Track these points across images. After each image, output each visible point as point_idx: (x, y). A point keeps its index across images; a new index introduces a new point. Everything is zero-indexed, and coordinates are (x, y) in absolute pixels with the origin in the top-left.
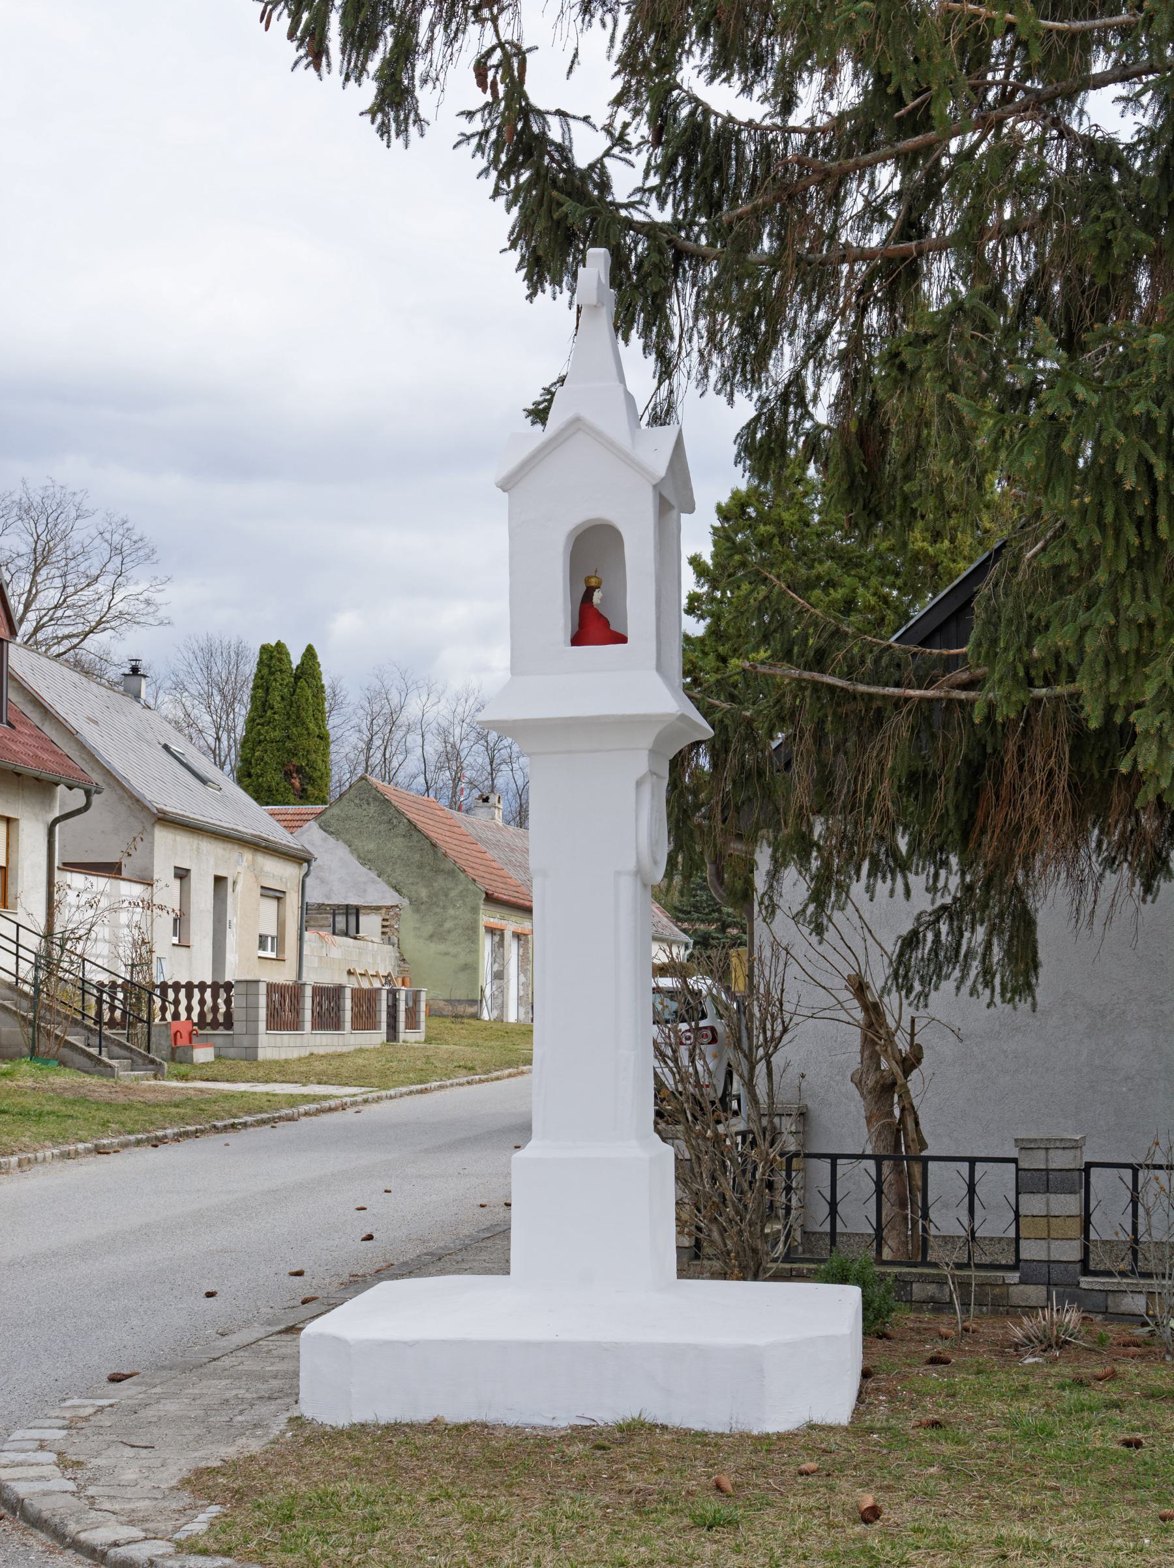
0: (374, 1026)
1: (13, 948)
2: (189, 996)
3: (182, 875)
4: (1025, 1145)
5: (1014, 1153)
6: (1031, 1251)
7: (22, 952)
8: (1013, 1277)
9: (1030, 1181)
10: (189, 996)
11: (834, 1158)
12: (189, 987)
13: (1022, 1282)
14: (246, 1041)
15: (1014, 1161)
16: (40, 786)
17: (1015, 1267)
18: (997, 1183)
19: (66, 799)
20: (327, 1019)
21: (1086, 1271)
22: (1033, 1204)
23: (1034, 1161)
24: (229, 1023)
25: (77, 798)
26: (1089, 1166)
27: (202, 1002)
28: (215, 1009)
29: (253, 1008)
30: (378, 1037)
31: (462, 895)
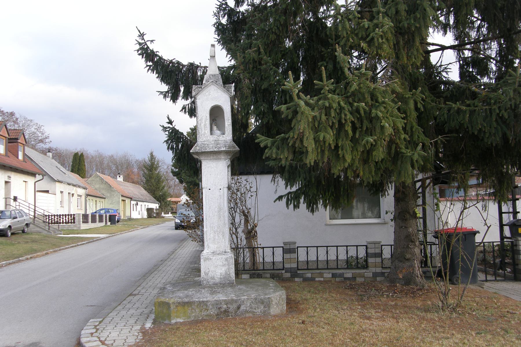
0: (102, 222)
1: (28, 208)
2: (66, 217)
3: (62, 192)
4: (285, 243)
5: (283, 245)
6: (287, 266)
7: (30, 209)
8: (284, 272)
9: (285, 251)
10: (66, 217)
11: (263, 248)
12: (66, 215)
13: (286, 272)
14: (78, 226)
15: (283, 247)
16: (33, 175)
17: (283, 269)
18: (279, 252)
19: (39, 177)
20: (94, 221)
21: (298, 269)
22: (287, 256)
23: (288, 247)
24: (74, 223)
25: (40, 177)
26: (298, 247)
27: (68, 218)
28: (66, 220)
29: (79, 219)
30: (103, 224)
31: (117, 195)
